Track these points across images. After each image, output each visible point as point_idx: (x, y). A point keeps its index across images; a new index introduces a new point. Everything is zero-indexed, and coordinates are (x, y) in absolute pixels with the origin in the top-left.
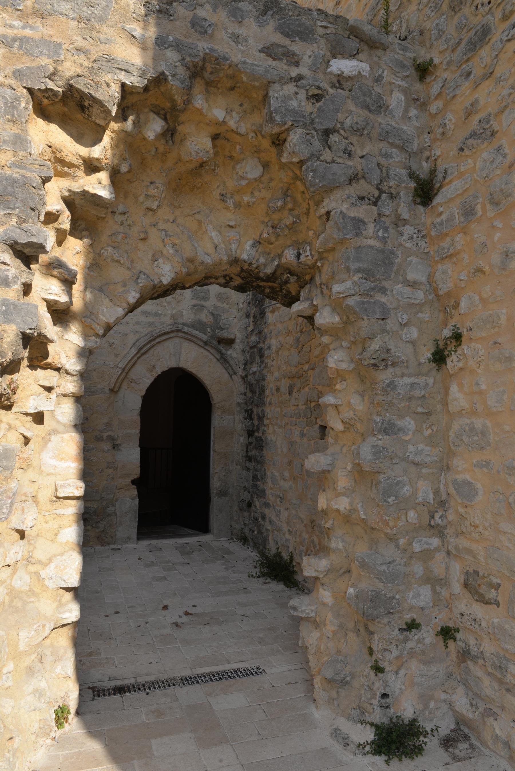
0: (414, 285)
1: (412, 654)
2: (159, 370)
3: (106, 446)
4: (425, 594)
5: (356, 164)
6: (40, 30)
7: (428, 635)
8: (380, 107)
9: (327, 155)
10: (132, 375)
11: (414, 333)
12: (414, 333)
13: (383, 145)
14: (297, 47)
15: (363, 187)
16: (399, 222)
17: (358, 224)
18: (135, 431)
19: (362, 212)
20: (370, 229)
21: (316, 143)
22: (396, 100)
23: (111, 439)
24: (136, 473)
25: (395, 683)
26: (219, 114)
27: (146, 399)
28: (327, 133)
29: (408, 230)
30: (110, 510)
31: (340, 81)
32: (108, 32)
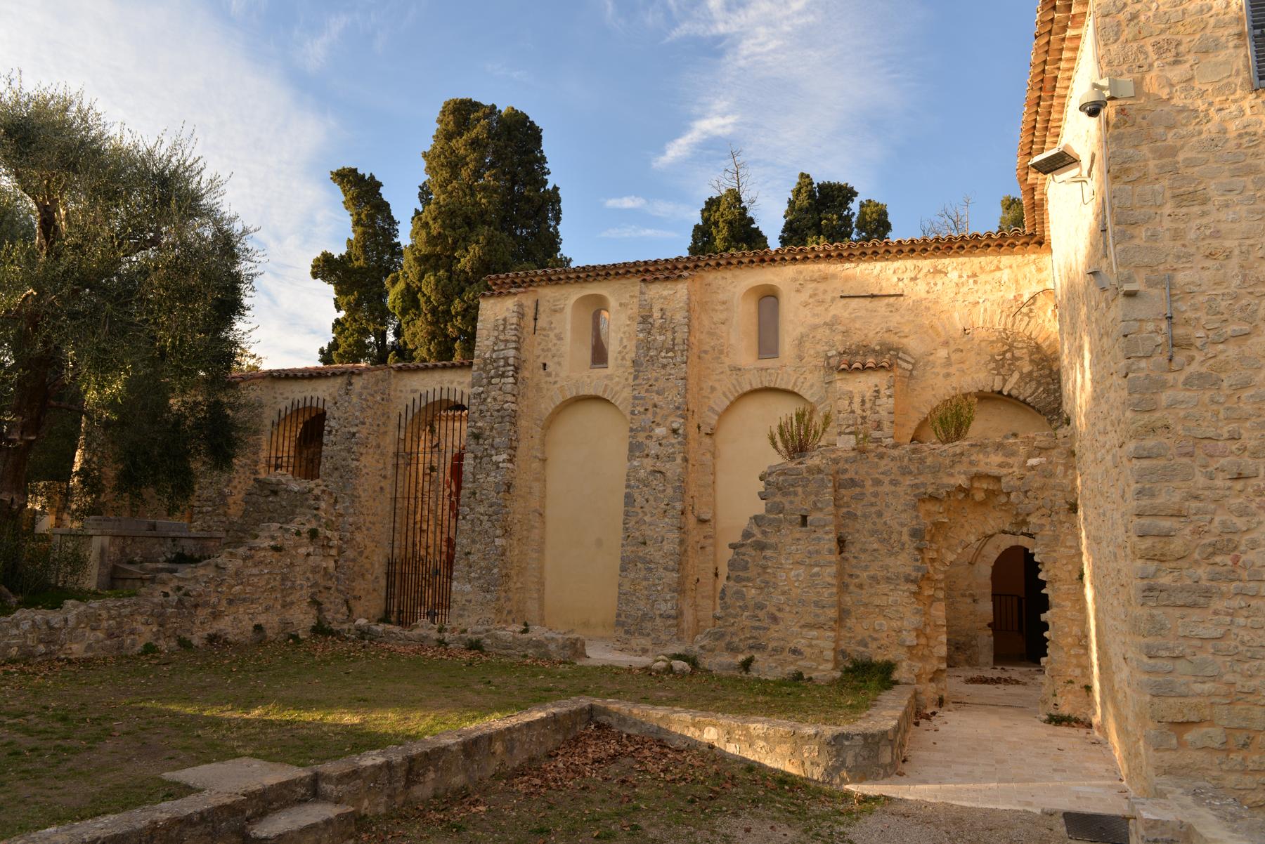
0: (1071, 547)
1: (1069, 692)
2: (1003, 548)
3: (969, 600)
4: (1078, 672)
5: (1040, 502)
6: (921, 479)
7: (1077, 687)
8: (1052, 475)
9: (1026, 501)
10: (984, 552)
11: (1070, 567)
12: (1070, 567)
13: (1054, 492)
14: (1010, 461)
15: (1044, 511)
16: (1061, 522)
17: (1042, 526)
18: (989, 591)
19: (1043, 521)
20: (1048, 527)
21: (1022, 497)
22: (1060, 469)
23: (971, 595)
24: (991, 619)
25: (1060, 701)
26: (985, 486)
27: (994, 568)
28: (1026, 492)
29: (1067, 525)
30: (974, 643)
31: (1033, 468)
32: (941, 474)
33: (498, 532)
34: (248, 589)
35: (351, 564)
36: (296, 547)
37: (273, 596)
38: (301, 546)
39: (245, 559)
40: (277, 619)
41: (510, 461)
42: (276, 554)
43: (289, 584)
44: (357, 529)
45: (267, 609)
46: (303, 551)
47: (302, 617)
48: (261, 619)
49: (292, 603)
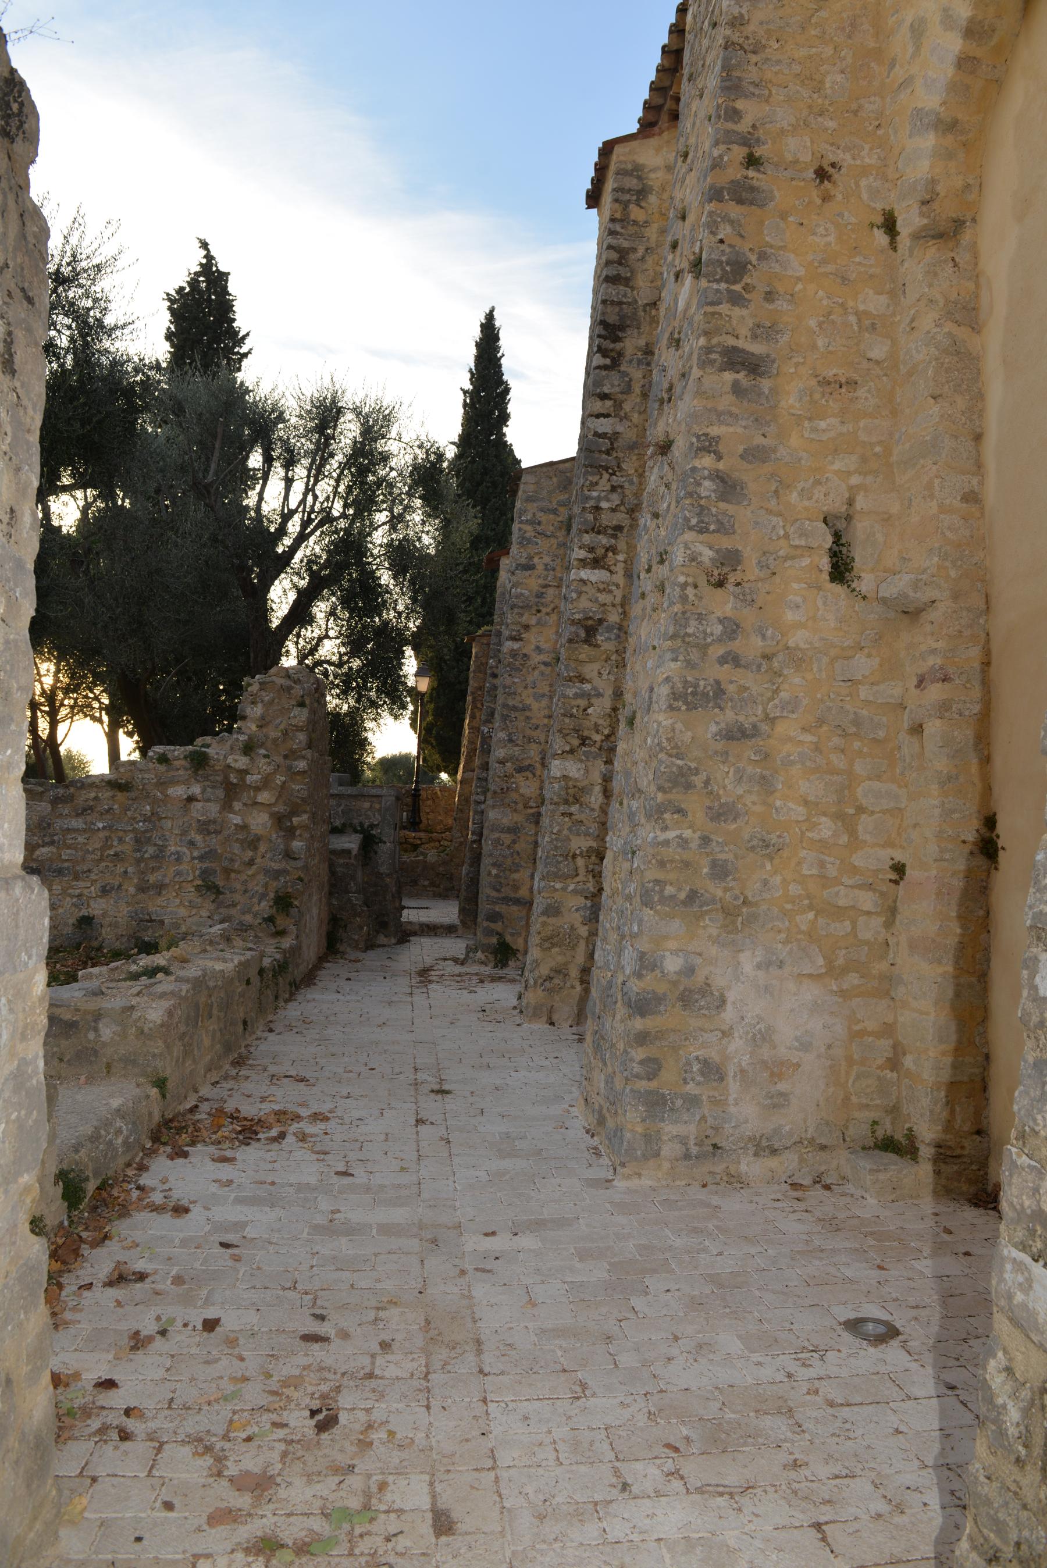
33: (558, 744)
34: (66, 854)
35: (507, 838)
36: (162, 784)
37: (120, 869)
38: (174, 782)
39: (55, 801)
40: (125, 910)
41: (596, 563)
42: (120, 796)
43: (151, 850)
44: (520, 770)
45: (105, 891)
46: (178, 791)
47: (183, 912)
48: (97, 908)
49: (160, 888)
